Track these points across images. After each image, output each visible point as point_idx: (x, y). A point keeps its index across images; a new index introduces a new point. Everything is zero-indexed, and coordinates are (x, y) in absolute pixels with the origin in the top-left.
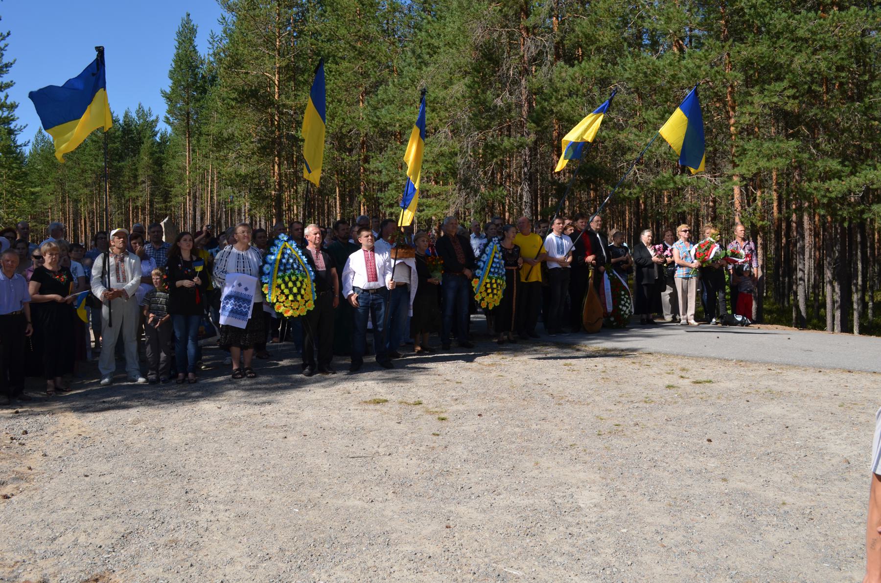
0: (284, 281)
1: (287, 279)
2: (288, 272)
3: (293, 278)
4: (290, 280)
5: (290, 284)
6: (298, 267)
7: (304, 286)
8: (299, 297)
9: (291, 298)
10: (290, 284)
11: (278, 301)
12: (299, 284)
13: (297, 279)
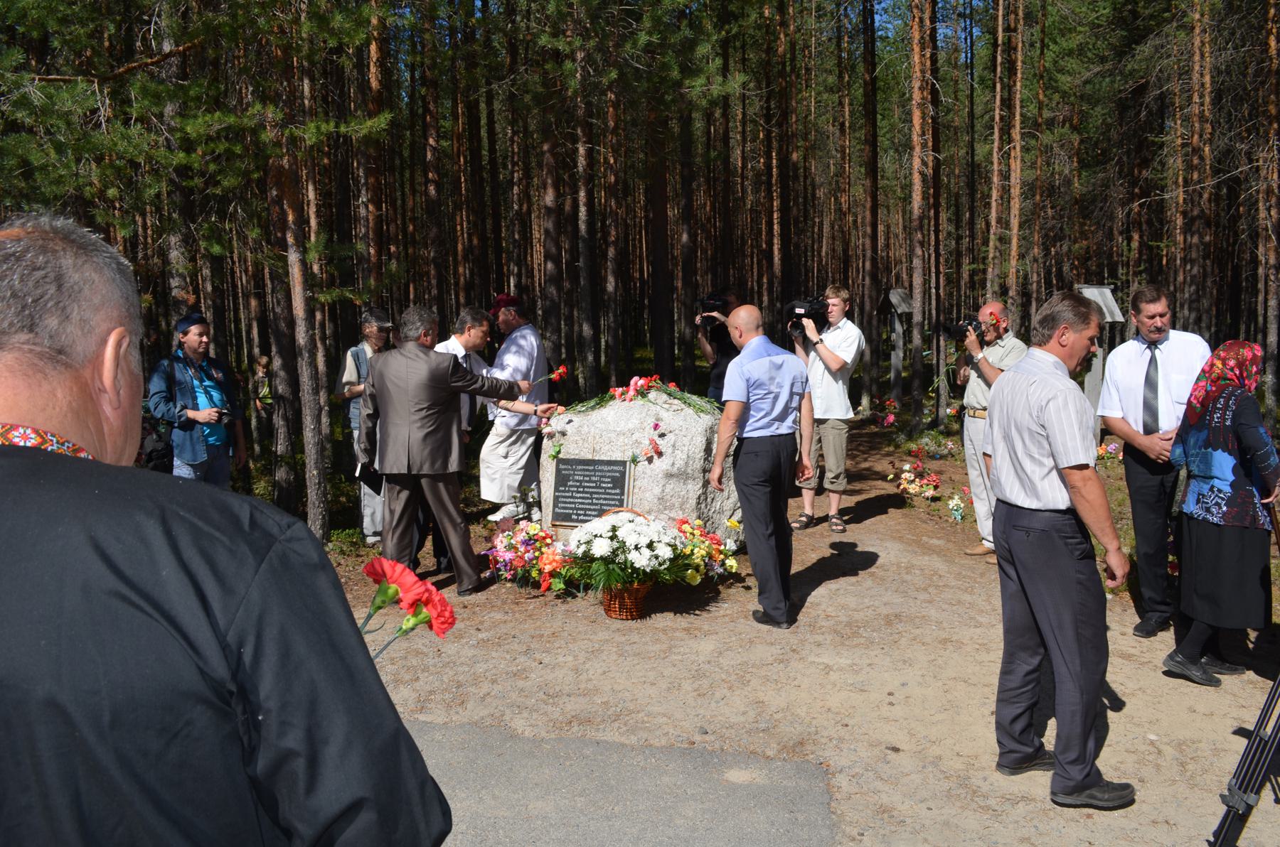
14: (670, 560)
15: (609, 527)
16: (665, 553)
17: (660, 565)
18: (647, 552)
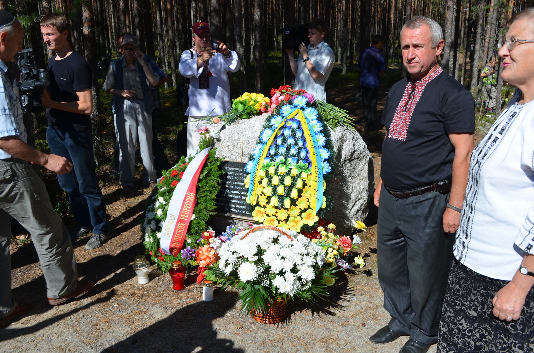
0: (267, 172)
1: (272, 170)
2: (280, 159)
3: (283, 170)
4: (276, 173)
5: (276, 180)
6: (299, 153)
7: (299, 184)
8: (287, 203)
9: (274, 201)
10: (276, 180)
11: (257, 204)
12: (288, 181)
13: (288, 173)
14: (313, 281)
15: (255, 251)
16: (308, 274)
17: (303, 285)
18: (290, 276)
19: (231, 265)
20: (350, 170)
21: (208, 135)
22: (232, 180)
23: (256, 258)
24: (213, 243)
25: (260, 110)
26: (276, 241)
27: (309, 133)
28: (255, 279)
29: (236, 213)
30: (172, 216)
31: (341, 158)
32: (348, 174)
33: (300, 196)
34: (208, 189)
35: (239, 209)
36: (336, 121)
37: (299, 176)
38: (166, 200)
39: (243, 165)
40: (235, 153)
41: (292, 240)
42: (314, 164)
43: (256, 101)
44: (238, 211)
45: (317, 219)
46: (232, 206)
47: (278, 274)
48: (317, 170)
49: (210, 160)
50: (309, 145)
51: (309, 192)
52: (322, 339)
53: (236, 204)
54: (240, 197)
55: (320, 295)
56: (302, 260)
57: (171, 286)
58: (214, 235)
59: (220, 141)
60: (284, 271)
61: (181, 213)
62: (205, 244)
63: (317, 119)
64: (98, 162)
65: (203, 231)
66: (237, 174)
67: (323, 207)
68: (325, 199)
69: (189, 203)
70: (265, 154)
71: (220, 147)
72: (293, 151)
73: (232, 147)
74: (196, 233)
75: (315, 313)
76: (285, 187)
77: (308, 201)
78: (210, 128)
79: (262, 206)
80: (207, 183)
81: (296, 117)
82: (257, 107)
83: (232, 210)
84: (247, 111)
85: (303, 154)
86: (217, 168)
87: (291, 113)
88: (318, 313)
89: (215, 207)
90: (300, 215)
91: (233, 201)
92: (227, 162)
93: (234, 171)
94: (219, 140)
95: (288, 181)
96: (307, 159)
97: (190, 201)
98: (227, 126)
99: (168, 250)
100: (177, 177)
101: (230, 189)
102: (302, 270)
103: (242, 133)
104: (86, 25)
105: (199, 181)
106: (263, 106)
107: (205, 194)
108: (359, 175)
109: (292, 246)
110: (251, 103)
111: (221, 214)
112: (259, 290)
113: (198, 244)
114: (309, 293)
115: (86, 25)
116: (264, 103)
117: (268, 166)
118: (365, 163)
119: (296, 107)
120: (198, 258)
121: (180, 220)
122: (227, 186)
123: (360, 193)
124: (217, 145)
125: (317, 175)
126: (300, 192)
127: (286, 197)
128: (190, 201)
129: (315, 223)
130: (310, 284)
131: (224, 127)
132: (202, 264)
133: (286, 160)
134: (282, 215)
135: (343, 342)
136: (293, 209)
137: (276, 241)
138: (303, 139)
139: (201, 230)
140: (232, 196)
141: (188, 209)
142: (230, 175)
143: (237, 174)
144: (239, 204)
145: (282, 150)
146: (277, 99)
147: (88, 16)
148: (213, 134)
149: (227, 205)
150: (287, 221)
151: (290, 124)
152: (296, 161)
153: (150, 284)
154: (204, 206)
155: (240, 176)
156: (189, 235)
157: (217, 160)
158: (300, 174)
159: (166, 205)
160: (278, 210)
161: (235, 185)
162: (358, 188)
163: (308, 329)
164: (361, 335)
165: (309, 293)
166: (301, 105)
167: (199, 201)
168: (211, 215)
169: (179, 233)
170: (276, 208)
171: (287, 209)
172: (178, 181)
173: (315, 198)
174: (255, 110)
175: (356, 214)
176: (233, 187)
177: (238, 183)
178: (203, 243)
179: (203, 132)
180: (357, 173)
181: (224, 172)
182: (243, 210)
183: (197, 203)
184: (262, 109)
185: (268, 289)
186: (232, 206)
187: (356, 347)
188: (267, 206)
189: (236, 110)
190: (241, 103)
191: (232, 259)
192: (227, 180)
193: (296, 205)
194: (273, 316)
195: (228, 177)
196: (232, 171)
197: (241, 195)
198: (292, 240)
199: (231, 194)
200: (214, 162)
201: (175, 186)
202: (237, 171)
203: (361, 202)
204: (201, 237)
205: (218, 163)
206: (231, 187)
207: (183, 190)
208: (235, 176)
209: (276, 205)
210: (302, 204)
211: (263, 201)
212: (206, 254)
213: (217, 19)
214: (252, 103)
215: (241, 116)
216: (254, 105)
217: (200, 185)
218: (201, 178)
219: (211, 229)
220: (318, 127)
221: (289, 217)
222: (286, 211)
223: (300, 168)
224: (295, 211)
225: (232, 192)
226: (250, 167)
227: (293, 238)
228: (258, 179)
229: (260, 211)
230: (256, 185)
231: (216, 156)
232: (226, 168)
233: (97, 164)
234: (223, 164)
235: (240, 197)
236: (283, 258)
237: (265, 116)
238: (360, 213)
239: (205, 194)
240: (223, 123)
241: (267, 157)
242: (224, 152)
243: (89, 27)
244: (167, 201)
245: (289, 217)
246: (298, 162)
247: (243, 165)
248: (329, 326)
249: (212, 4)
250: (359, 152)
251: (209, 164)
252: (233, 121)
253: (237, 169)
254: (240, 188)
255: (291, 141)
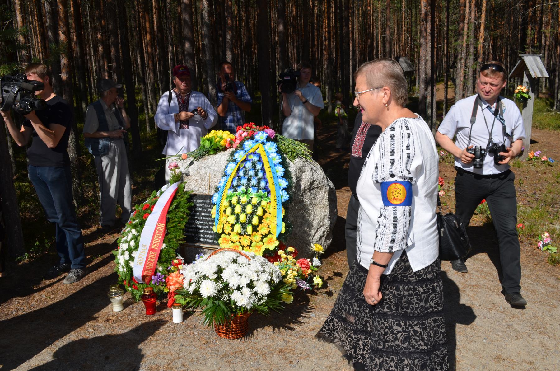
0: (230, 201)
1: (234, 200)
2: (242, 189)
3: (244, 199)
4: (238, 202)
5: (238, 209)
6: (259, 183)
7: (260, 212)
8: (249, 229)
10: (238, 209)
11: (223, 232)
12: (249, 209)
13: (249, 202)
14: (268, 295)
15: (215, 269)
16: (263, 289)
17: (259, 300)
18: (247, 291)
19: (194, 284)
20: (310, 198)
21: (177, 171)
22: (200, 212)
23: (217, 275)
24: (182, 270)
25: (225, 146)
26: (234, 261)
27: (269, 164)
28: (215, 295)
29: (205, 243)
30: (144, 246)
31: (300, 188)
32: (308, 203)
33: (260, 222)
34: (176, 220)
35: (208, 238)
36: (295, 154)
37: (259, 204)
38: (138, 232)
39: (210, 197)
40: (202, 187)
41: (250, 260)
42: (272, 193)
43: (222, 138)
44: (207, 240)
45: (277, 243)
46: (201, 236)
47: (236, 290)
48: (276, 198)
49: (179, 194)
50: (268, 176)
51: (269, 218)
52: (279, 350)
53: (205, 234)
54: (208, 227)
55: (276, 309)
56: (258, 276)
57: (144, 312)
58: (183, 261)
59: (189, 175)
60: (241, 286)
61: (152, 243)
62: (175, 271)
63: (276, 152)
64: (77, 203)
65: (173, 258)
66: (205, 206)
67: (283, 232)
68: (284, 225)
69: (159, 234)
70: (229, 185)
71: (189, 181)
72: (254, 182)
73: (200, 181)
74: (167, 261)
75: (276, 329)
76: (247, 215)
77: (269, 227)
78: (180, 164)
79: (227, 233)
80: (176, 214)
81: (257, 151)
82: (222, 143)
83: (202, 239)
84: (213, 147)
85: (263, 184)
86: (186, 201)
87: (252, 147)
88: (279, 329)
89: (183, 237)
90: (262, 241)
91: (202, 231)
92: (195, 195)
93: (202, 203)
94: (187, 175)
95: (249, 209)
96: (266, 189)
97: (160, 231)
98: (195, 162)
99: (141, 278)
100: (148, 210)
101: (199, 220)
102: (258, 285)
103: (209, 168)
104: (64, 71)
105: (169, 212)
106: (228, 142)
107: (174, 224)
108: (320, 203)
109: (249, 264)
110: (217, 140)
111: (191, 244)
112: (219, 305)
113: (169, 272)
114: (266, 307)
115: (64, 71)
116: (229, 139)
117: (231, 196)
118: (325, 192)
119: (257, 141)
120: (168, 284)
121: (151, 250)
122: (196, 218)
123: (322, 220)
124: (186, 180)
125: (276, 203)
126: (261, 219)
127: (248, 224)
128: (160, 231)
129: (276, 247)
130: (266, 298)
131: (192, 163)
132: (172, 288)
133: (247, 190)
134: (246, 241)
135: (299, 352)
136: (255, 235)
137: (234, 261)
138: (263, 170)
139: (171, 258)
140: (200, 227)
141: (159, 239)
142: (198, 207)
143: (205, 206)
144: (208, 234)
145: (244, 181)
146: (241, 135)
147: (65, 62)
148: (182, 169)
149: (196, 235)
150: (250, 246)
151: (251, 157)
152: (256, 191)
153: (124, 311)
154: (173, 236)
155: (208, 207)
156: (160, 263)
157: (186, 193)
158: (260, 202)
159: (138, 236)
160: (241, 237)
161: (203, 216)
162: (319, 216)
163: (268, 342)
164: (315, 345)
165: (266, 307)
166: (262, 140)
167: (169, 231)
168: (180, 244)
169: (151, 262)
170: (240, 234)
171: (249, 235)
172: (149, 214)
173: (275, 223)
174: (221, 146)
175: (319, 240)
176: (201, 218)
177: (206, 214)
178: (173, 269)
179: (173, 168)
180: (317, 202)
181: (192, 204)
182: (211, 239)
183: (166, 234)
184: (227, 145)
185: (228, 303)
186: (201, 236)
187: (310, 355)
188: (232, 233)
189: (204, 146)
190: (208, 140)
191: (195, 278)
192: (196, 212)
193: (257, 231)
194: (236, 331)
195: (197, 209)
196: (200, 203)
197: (209, 225)
198: (250, 260)
199: (200, 224)
200: (183, 195)
201: (146, 219)
202: (205, 203)
203: (323, 229)
204: (171, 265)
205: (187, 196)
206: (199, 218)
207: (154, 221)
208: (203, 208)
209: (240, 232)
210: (263, 230)
211: (228, 229)
212: (175, 279)
213: (191, 62)
214: (218, 139)
215: (208, 152)
216: (219, 142)
217: (169, 217)
218: (170, 210)
219: (180, 256)
220: (277, 159)
221: (251, 242)
222: (248, 237)
223: (260, 196)
224: (258, 237)
225: (201, 222)
226: (215, 199)
227: (251, 258)
228: (223, 209)
229: (225, 239)
230: (221, 214)
231: (185, 190)
232: (195, 201)
233: (76, 205)
234: (192, 197)
235: (208, 227)
236: (240, 275)
237: (230, 151)
238: (323, 239)
239: (174, 224)
240: (192, 159)
241: (230, 188)
242: (192, 186)
243: (67, 72)
244: (139, 232)
245: (251, 242)
246: (257, 192)
247: (210, 197)
248: (288, 339)
249: (186, 49)
250: (318, 181)
251: (178, 197)
252: (201, 157)
253: (205, 201)
254: (208, 219)
255: (251, 173)
